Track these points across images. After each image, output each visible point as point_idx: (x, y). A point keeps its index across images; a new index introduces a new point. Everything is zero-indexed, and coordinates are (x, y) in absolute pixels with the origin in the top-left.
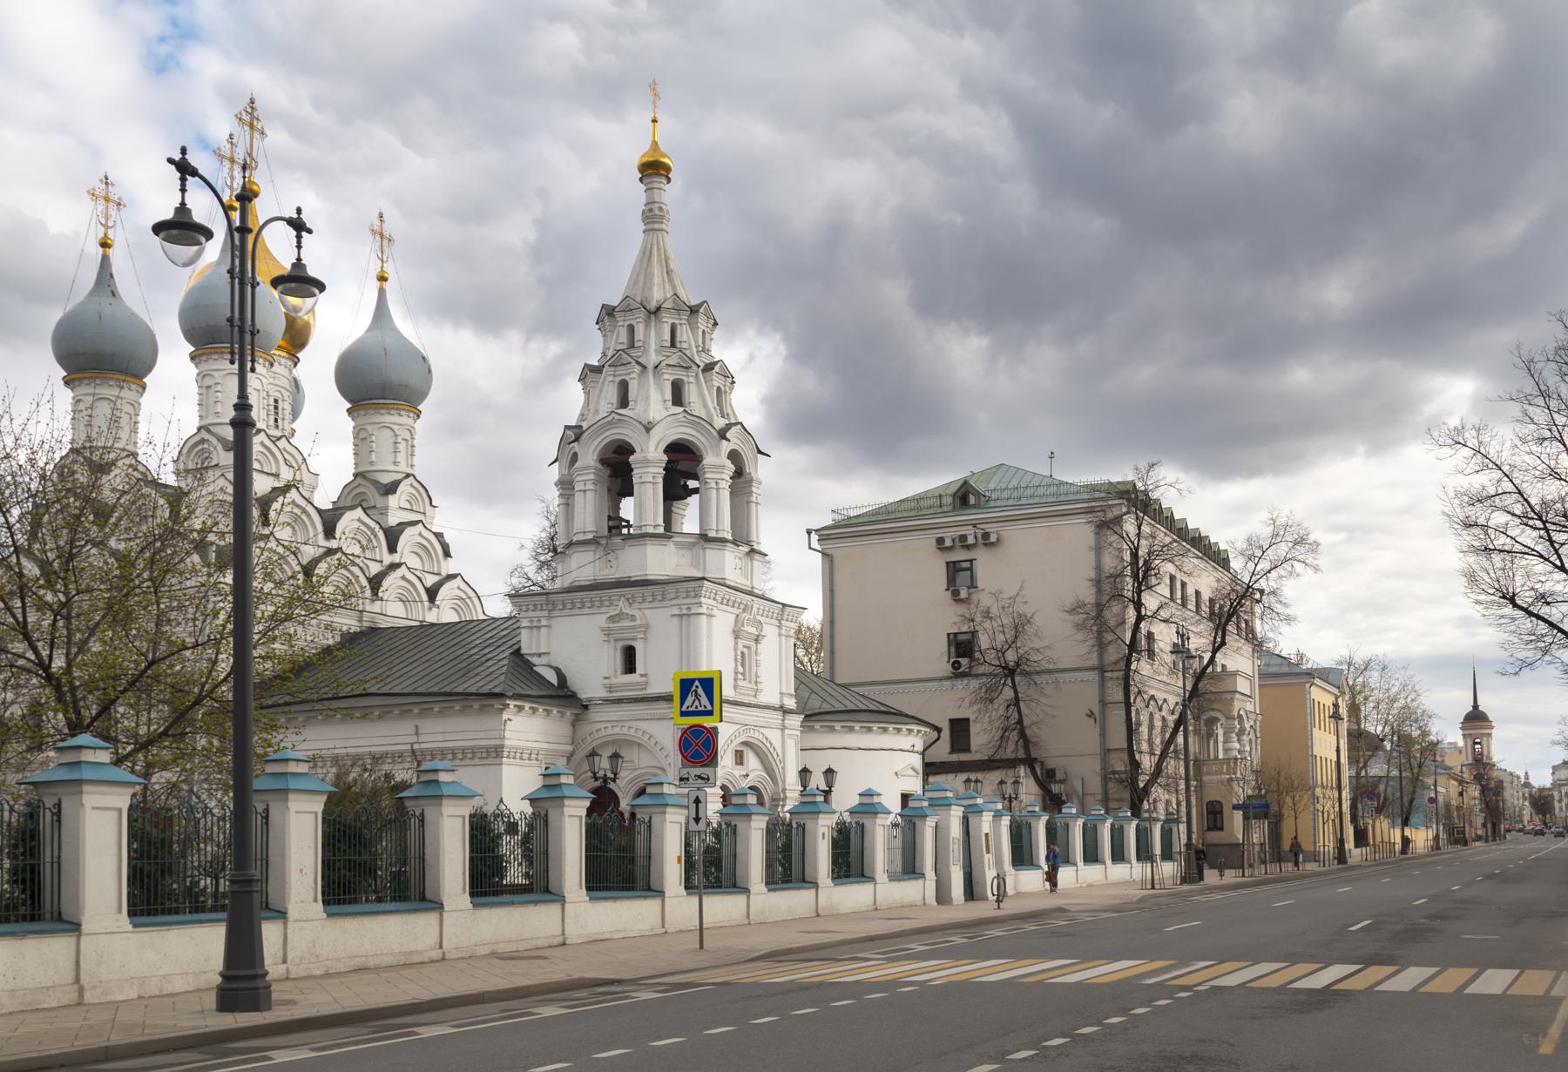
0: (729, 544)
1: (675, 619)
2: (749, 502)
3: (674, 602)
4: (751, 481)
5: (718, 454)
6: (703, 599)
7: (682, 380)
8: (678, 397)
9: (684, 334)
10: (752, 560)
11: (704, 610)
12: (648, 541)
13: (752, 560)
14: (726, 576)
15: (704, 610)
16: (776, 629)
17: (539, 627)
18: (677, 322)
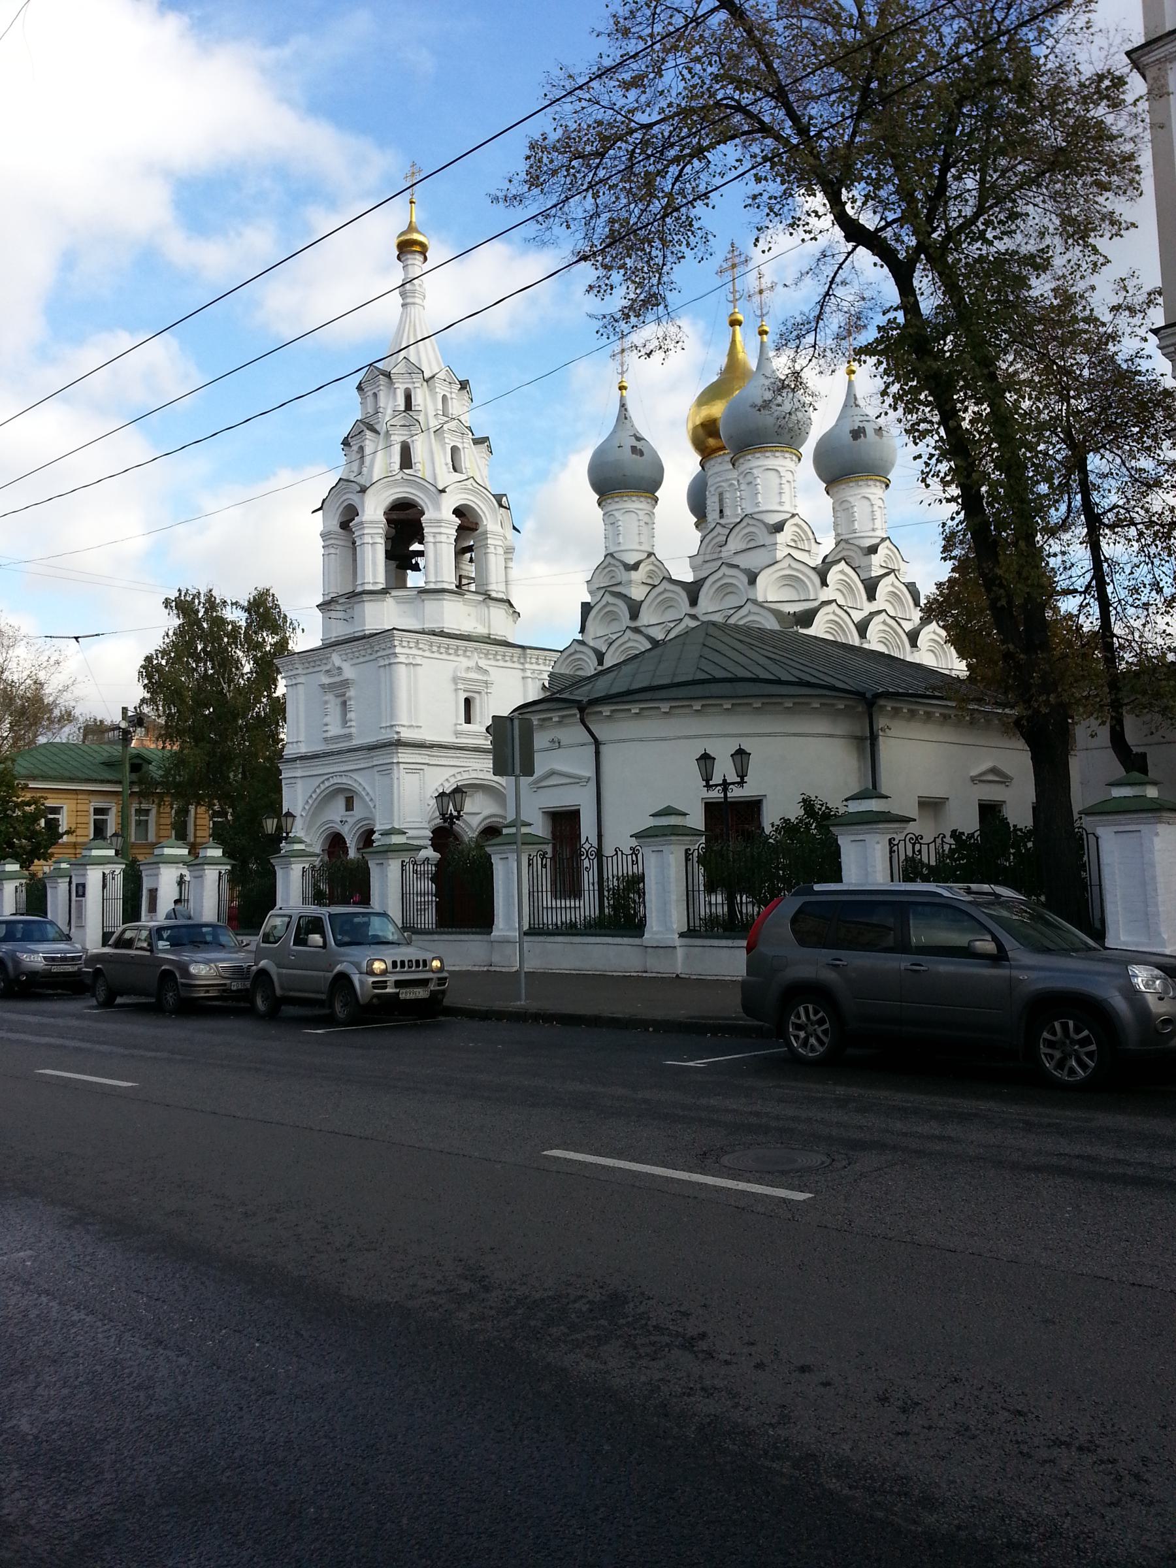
0: (447, 596)
1: (382, 669)
2: (486, 553)
3: (379, 654)
4: (486, 532)
5: (438, 507)
6: (398, 650)
7: (458, 448)
8: (406, 461)
9: (418, 399)
10: (488, 607)
11: (402, 659)
12: (365, 597)
13: (488, 607)
14: (445, 625)
15: (402, 659)
16: (520, 674)
17: (296, 684)
18: (410, 386)
